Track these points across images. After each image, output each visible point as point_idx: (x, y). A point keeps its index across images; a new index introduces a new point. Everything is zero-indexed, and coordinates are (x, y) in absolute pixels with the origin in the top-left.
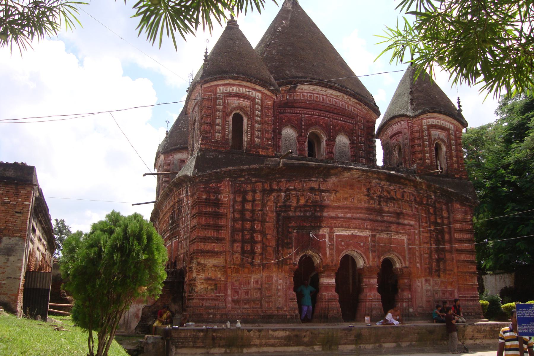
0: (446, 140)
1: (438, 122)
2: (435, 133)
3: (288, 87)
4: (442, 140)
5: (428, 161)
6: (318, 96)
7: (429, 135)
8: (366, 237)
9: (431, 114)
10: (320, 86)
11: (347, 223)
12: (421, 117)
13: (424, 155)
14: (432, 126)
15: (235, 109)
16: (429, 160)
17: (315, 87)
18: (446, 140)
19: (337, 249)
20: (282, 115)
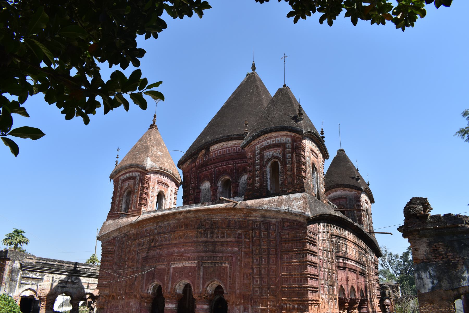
0: (281, 156)
1: (273, 141)
2: (269, 153)
3: (204, 151)
4: (277, 157)
5: (258, 185)
6: (226, 149)
7: (262, 158)
8: (194, 268)
9: (263, 137)
10: (224, 141)
11: (180, 258)
12: (253, 143)
13: (254, 180)
14: (263, 149)
15: (127, 188)
16: (258, 182)
17: (221, 144)
18: (281, 156)
19: (173, 278)
20: (200, 174)
